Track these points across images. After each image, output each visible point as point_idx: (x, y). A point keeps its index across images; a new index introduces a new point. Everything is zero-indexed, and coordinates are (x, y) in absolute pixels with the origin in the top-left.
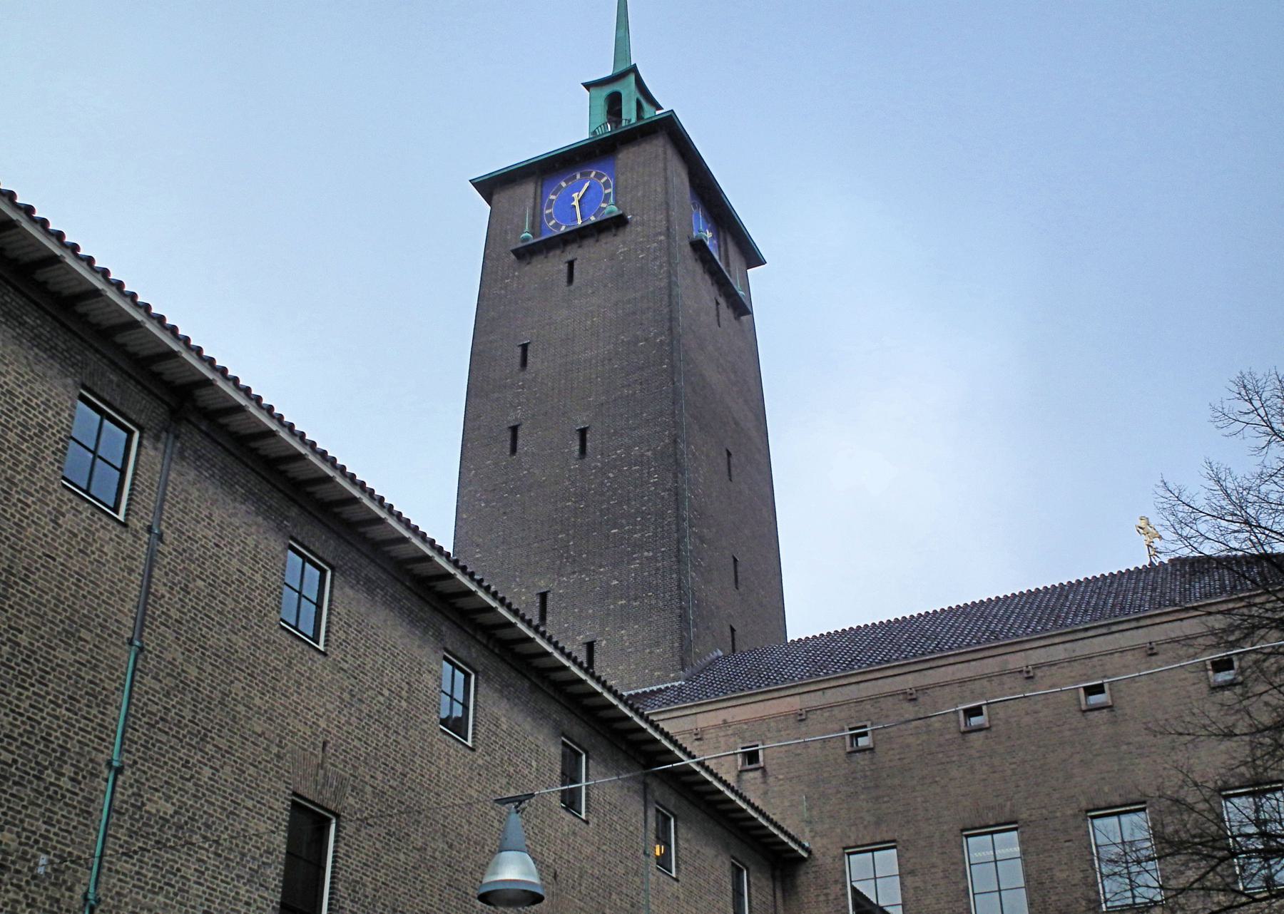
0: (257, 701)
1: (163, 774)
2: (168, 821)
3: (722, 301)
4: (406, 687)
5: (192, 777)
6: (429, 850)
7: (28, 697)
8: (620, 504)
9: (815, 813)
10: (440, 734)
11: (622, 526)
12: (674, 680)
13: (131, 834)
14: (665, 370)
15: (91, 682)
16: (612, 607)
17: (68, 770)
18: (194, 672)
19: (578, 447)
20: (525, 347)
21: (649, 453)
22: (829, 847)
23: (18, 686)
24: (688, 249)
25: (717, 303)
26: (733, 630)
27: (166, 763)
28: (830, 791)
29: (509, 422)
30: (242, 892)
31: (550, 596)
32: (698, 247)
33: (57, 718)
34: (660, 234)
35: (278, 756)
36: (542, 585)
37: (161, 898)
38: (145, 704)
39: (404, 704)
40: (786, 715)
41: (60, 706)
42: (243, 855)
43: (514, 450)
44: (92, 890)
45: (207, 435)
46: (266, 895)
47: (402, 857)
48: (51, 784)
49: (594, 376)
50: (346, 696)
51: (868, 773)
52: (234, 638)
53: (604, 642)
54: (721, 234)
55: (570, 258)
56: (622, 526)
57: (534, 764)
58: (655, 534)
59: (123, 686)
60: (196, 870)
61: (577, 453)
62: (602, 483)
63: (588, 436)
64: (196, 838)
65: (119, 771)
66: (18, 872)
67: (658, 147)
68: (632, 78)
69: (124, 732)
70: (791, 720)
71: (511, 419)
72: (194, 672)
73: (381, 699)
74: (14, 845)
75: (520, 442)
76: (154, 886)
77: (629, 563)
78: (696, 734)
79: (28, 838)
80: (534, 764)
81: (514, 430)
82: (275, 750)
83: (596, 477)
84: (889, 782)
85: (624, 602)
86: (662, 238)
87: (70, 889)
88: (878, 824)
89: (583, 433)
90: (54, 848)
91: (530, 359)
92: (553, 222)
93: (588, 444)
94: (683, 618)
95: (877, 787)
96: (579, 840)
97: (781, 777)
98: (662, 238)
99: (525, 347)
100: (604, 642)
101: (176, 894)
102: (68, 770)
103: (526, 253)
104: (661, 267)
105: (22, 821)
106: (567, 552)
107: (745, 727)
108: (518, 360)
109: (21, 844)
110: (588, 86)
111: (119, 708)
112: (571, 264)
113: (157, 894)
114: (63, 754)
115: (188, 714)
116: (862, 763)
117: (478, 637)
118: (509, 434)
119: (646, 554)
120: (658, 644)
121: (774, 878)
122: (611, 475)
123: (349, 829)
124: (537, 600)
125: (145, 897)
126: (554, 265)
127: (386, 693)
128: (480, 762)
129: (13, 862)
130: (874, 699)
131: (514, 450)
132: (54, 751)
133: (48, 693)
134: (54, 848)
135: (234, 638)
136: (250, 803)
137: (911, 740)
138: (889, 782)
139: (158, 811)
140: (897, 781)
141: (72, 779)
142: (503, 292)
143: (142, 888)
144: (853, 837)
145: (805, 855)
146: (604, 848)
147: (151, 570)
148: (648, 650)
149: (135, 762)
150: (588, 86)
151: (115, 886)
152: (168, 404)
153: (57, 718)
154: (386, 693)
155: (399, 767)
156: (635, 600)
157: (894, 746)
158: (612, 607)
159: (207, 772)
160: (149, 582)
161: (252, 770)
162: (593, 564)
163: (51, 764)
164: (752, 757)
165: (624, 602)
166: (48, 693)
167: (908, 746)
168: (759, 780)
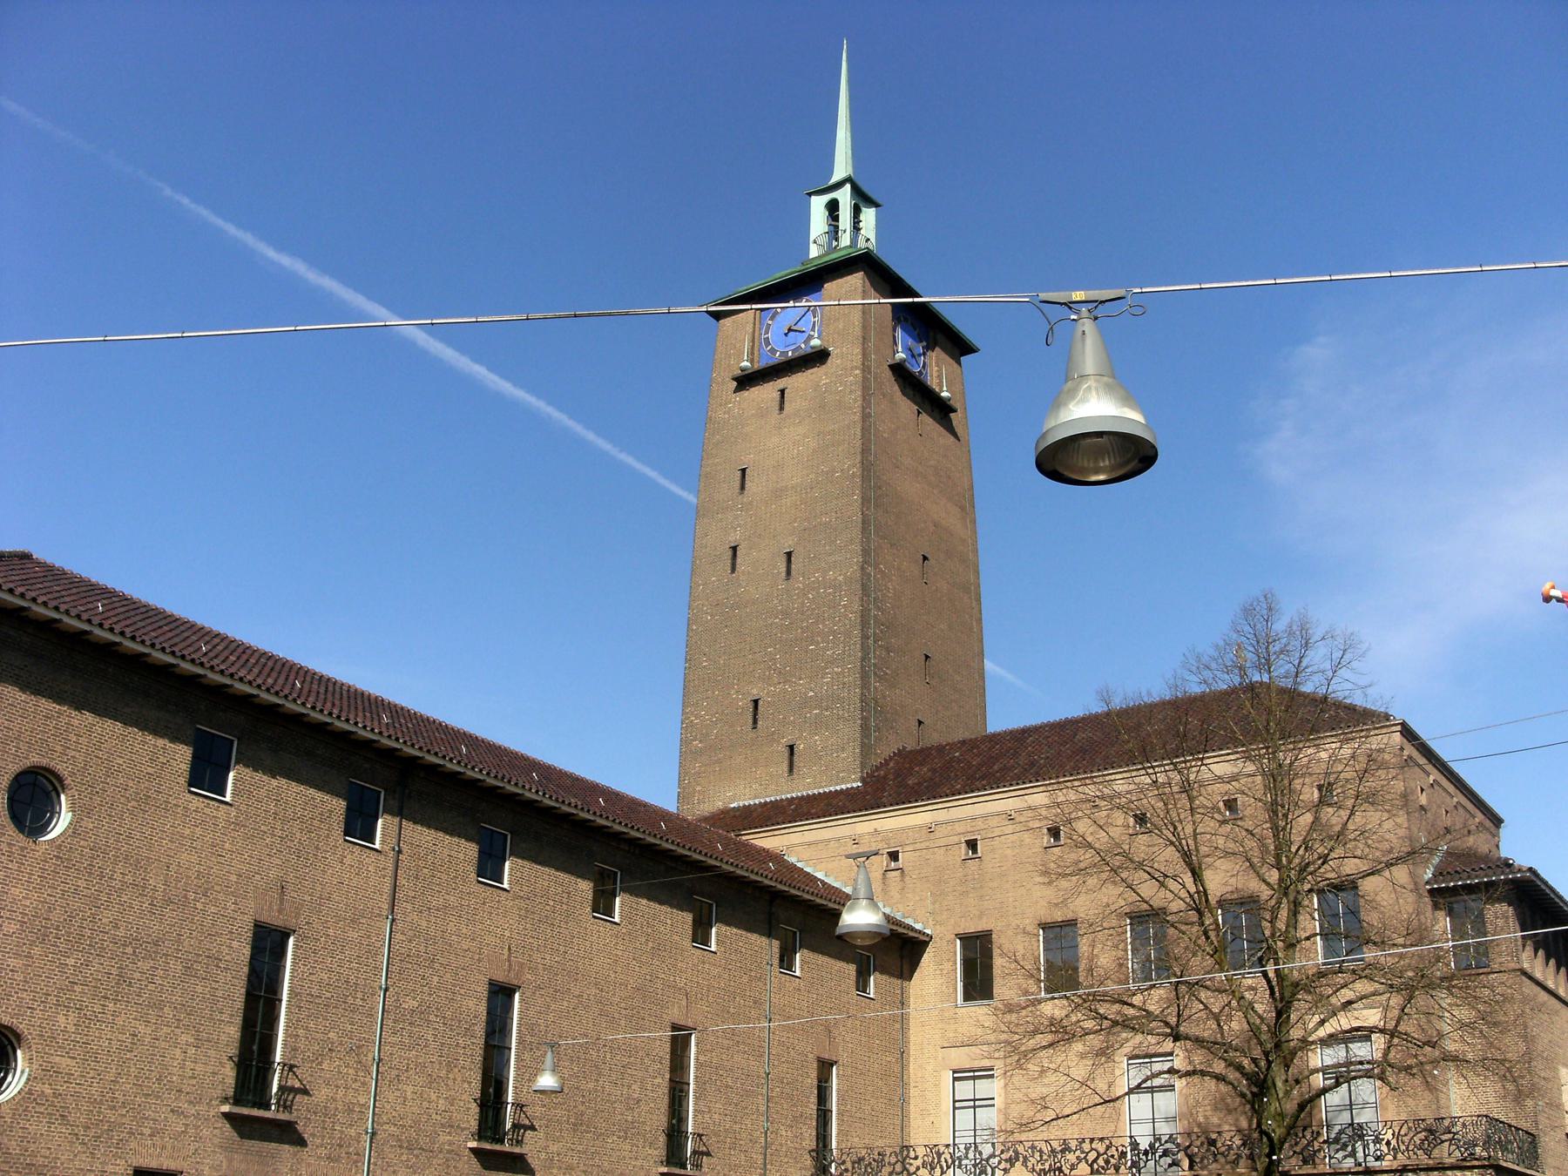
0: (464, 931)
1: (411, 986)
2: (415, 1011)
4: (565, 895)
5: (427, 984)
6: (585, 996)
7: (336, 962)
8: (817, 623)
9: (937, 906)
10: (592, 919)
11: (818, 643)
12: (854, 781)
13: (395, 1021)
14: (856, 501)
15: (367, 945)
16: (808, 715)
17: (359, 995)
18: (424, 924)
19: (785, 569)
20: (743, 471)
21: (841, 578)
22: (946, 933)
23: (331, 957)
24: (888, 373)
27: (411, 980)
28: (949, 890)
29: (730, 542)
30: (460, 1042)
31: (760, 703)
33: (351, 969)
34: (856, 368)
35: (479, 960)
36: (755, 692)
37: (413, 1052)
38: (398, 950)
39: (565, 907)
41: (352, 962)
42: (460, 1021)
43: (733, 569)
44: (376, 1054)
46: (475, 1041)
47: (565, 1003)
48: (352, 1004)
49: (798, 503)
50: (523, 913)
51: (977, 876)
52: (447, 897)
53: (802, 746)
54: (931, 334)
55: (781, 387)
56: (818, 643)
57: (669, 922)
59: (384, 942)
60: (433, 1034)
61: (784, 574)
62: (803, 603)
63: (792, 559)
64: (431, 1017)
65: (386, 990)
66: (339, 1051)
67: (856, 280)
68: (848, 186)
69: (388, 967)
70: (925, 831)
71: (733, 538)
74: (336, 1038)
75: (739, 560)
76: (410, 1047)
77: (822, 677)
78: (854, 840)
79: (343, 1034)
80: (669, 922)
81: (734, 549)
82: (477, 957)
83: (798, 598)
84: (991, 884)
85: (815, 712)
86: (857, 372)
87: (365, 1056)
88: (980, 917)
89: (789, 555)
90: (356, 1036)
91: (748, 484)
93: (793, 566)
94: (865, 728)
95: (981, 887)
96: (707, 966)
97: (914, 876)
98: (857, 372)
100: (802, 746)
101: (422, 1049)
102: (359, 995)
104: (855, 400)
105: (339, 1026)
106: (775, 664)
107: (891, 835)
108: (737, 484)
109: (340, 1037)
111: (383, 956)
112: (782, 392)
113: (412, 1051)
114: (356, 987)
115: (422, 949)
116: (973, 868)
117: (622, 847)
118: (730, 553)
119: (836, 669)
120: (843, 749)
121: (902, 958)
122: (810, 596)
124: (751, 706)
125: (405, 1053)
126: (766, 393)
127: (551, 903)
128: (624, 930)
129: (336, 1047)
130: (985, 817)
131: (733, 569)
132: (351, 987)
133: (345, 957)
134: (356, 1036)
135: (447, 897)
136: (462, 991)
137: (1009, 852)
138: (991, 884)
139: (409, 1006)
140: (995, 884)
141: (361, 999)
142: (727, 416)
143: (403, 1049)
144: (962, 926)
145: (927, 939)
146: (730, 967)
147: (396, 872)
148: (835, 755)
149: (395, 983)
151: (389, 1050)
153: (351, 969)
154: (551, 903)
157: (996, 856)
158: (808, 715)
159: (436, 979)
160: (396, 879)
161: (464, 973)
162: (795, 676)
163: (351, 994)
166: (345, 957)
167: (1006, 856)
168: (899, 879)
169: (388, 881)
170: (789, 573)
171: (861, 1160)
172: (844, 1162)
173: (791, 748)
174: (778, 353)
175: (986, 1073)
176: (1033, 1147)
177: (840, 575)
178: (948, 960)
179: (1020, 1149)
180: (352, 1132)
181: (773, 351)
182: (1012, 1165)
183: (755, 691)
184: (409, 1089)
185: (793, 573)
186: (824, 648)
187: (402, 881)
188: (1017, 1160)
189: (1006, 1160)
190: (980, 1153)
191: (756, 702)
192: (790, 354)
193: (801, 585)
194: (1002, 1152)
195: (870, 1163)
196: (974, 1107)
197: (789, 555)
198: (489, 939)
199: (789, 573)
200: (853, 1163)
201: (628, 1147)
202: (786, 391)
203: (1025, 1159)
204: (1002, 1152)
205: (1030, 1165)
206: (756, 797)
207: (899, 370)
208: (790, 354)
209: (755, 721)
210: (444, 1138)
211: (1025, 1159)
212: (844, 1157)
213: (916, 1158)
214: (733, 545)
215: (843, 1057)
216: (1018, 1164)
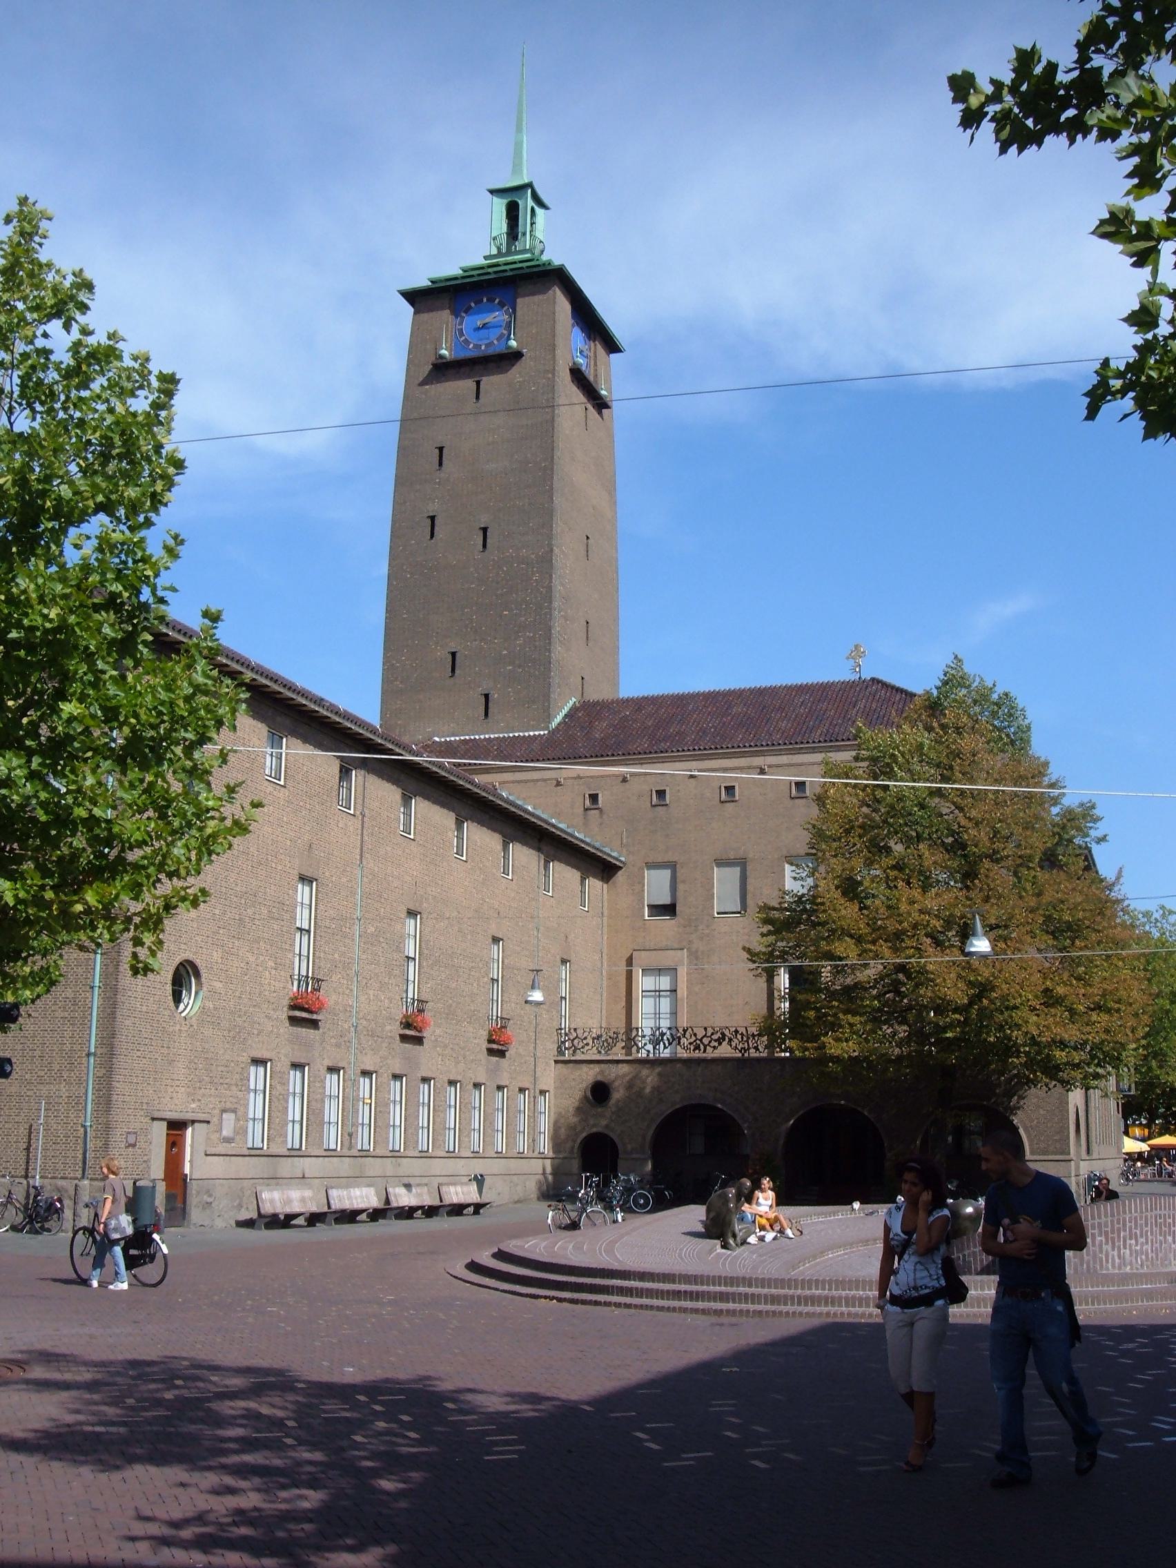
18: (376, 869)
20: (441, 449)
31: (458, 655)
32: (578, 375)
40: (617, 776)
43: (432, 536)
58: (535, 620)
64: (382, 940)
68: (529, 191)
71: (432, 508)
72: (376, 869)
75: (436, 529)
77: (516, 639)
81: (433, 518)
89: (485, 530)
99: (441, 449)
103: (443, 370)
112: (478, 383)
123: (424, 916)
131: (432, 536)
155: (440, 882)
156: (519, 667)
164: (594, 798)
168: (598, 815)
169: (359, 837)
170: (484, 546)
171: (599, 1037)
172: (585, 1038)
173: (487, 696)
175: (672, 971)
176: (736, 1032)
178: (639, 883)
179: (727, 1032)
180: (346, 1026)
181: (467, 342)
182: (720, 1044)
183: (452, 644)
184: (371, 992)
185: (488, 545)
186: (516, 614)
187: (366, 838)
188: (724, 1040)
189: (715, 1041)
190: (695, 1035)
191: (454, 654)
194: (712, 1034)
195: (606, 1040)
196: (659, 996)
197: (485, 530)
198: (408, 878)
199: (484, 546)
200: (594, 1039)
201: (471, 1029)
203: (730, 1040)
204: (712, 1034)
205: (733, 1044)
206: (453, 735)
207: (578, 375)
208: (483, 347)
209: (453, 670)
210: (388, 1028)
211: (730, 1040)
212: (586, 1034)
213: (643, 1036)
215: (573, 959)
216: (725, 1043)
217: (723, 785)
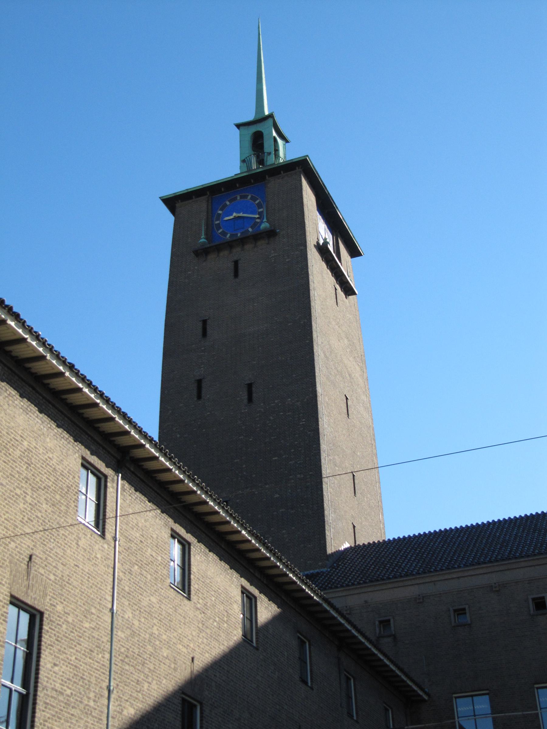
3: (338, 287)
4: (226, 614)
18: (136, 623)
19: (246, 397)
20: (205, 322)
21: (299, 403)
25: (336, 289)
26: (354, 527)
43: (199, 397)
45: (133, 473)
50: (200, 625)
57: (286, 654)
61: (246, 401)
63: (253, 389)
72: (136, 623)
73: (215, 624)
85: (283, 510)
89: (250, 387)
92: (221, 231)
99: (205, 322)
110: (238, 126)
112: (236, 263)
117: (256, 575)
119: (299, 476)
122: (271, 418)
131: (199, 397)
141: (94, 701)
142: (187, 281)
145: (426, 697)
148: (302, 545)
150: (238, 126)
152: (114, 457)
159: (146, 685)
165: (283, 510)
170: (250, 399)
174: (229, 235)
177: (298, 401)
192: (239, 235)
193: (262, 410)
197: (250, 387)
199: (250, 399)
202: (240, 262)
208: (239, 235)
214: (198, 378)
217: (530, 597)
